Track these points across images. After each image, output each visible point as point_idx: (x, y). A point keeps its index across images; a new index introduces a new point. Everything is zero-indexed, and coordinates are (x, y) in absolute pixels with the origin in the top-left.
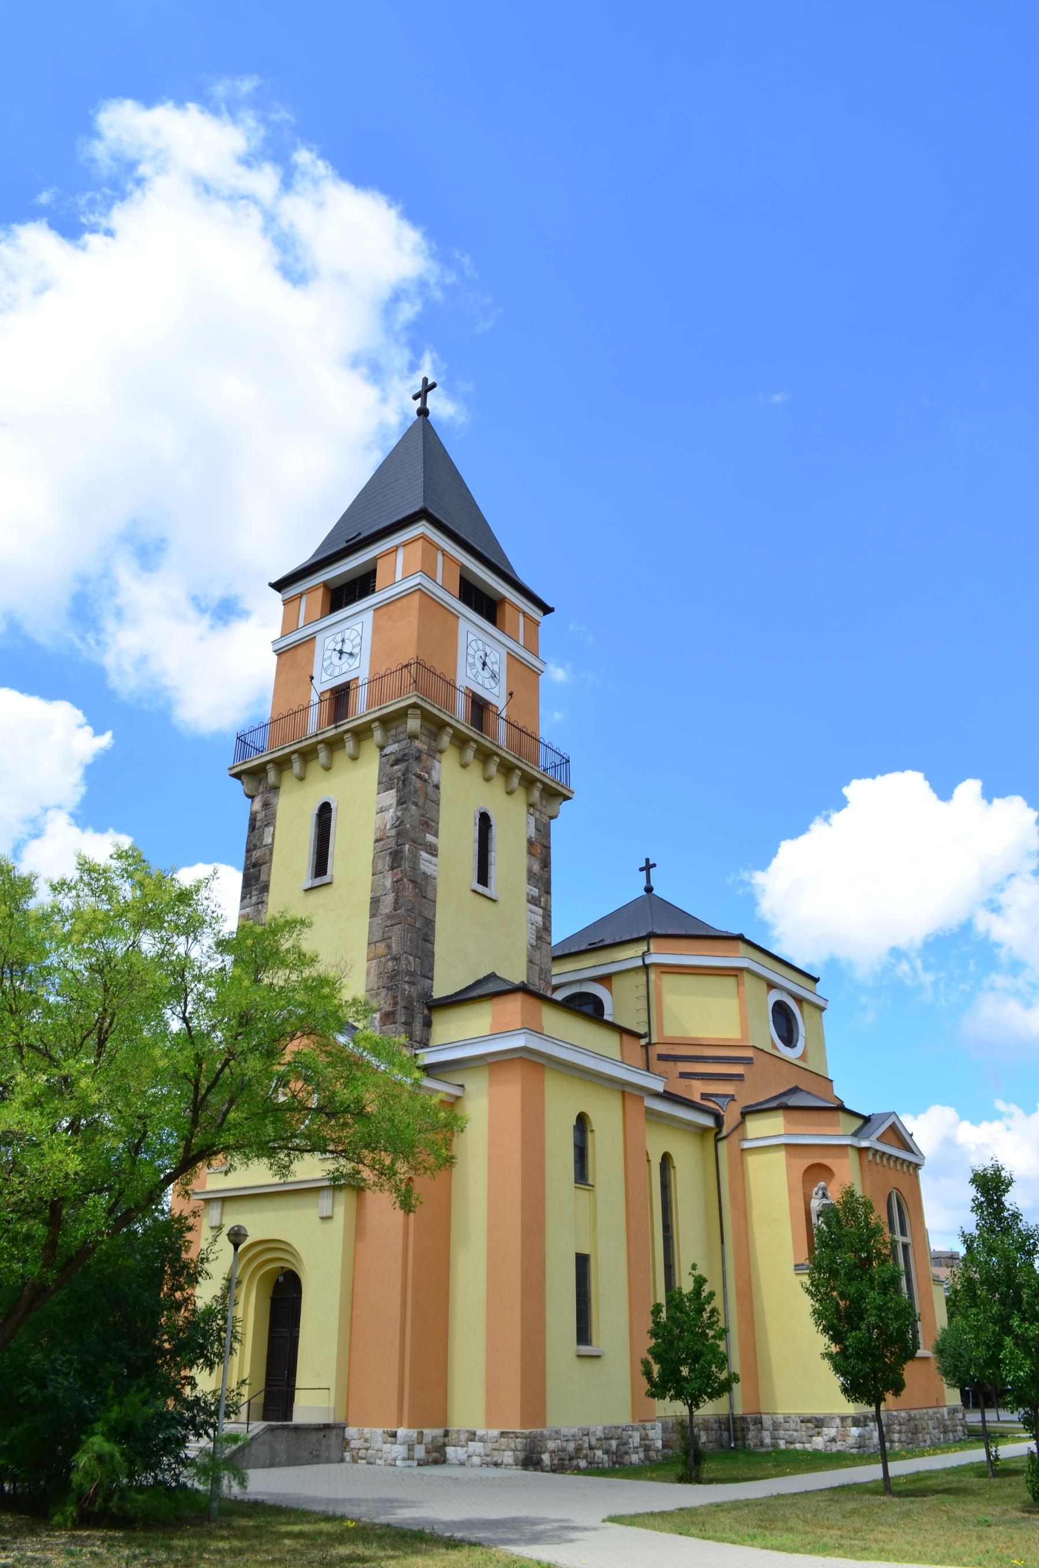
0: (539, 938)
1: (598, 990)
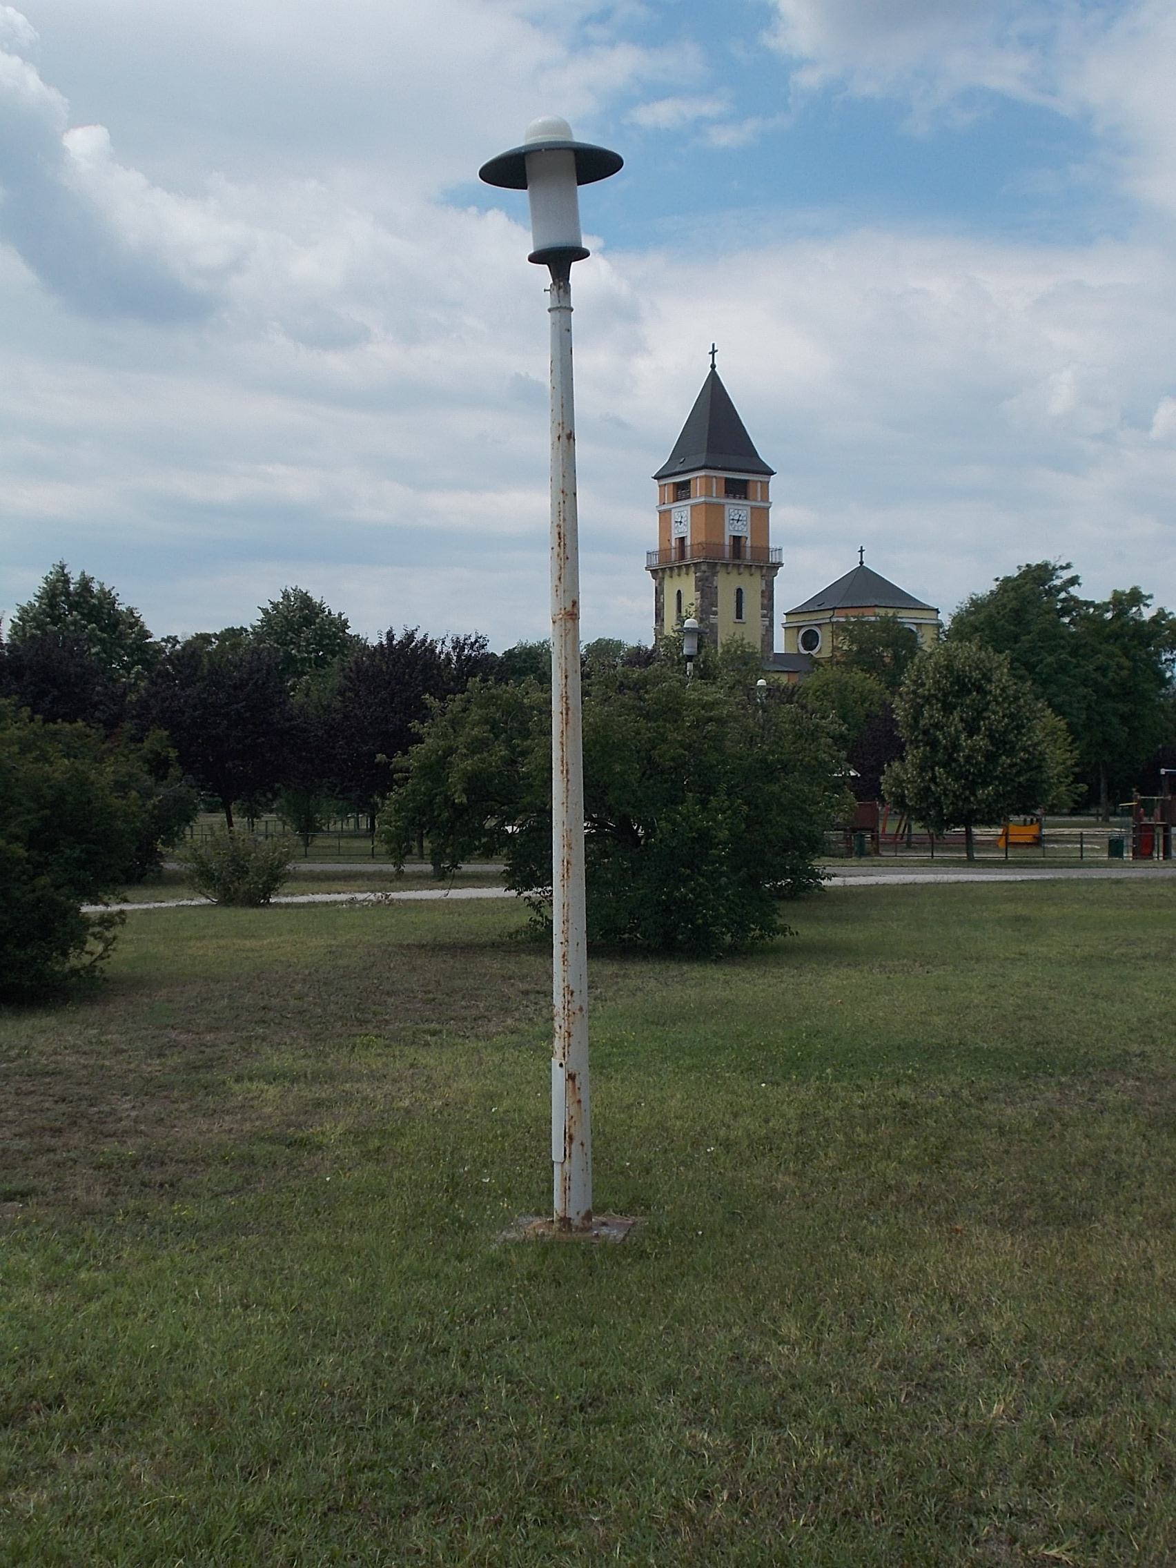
0: (767, 631)
1: (816, 629)
